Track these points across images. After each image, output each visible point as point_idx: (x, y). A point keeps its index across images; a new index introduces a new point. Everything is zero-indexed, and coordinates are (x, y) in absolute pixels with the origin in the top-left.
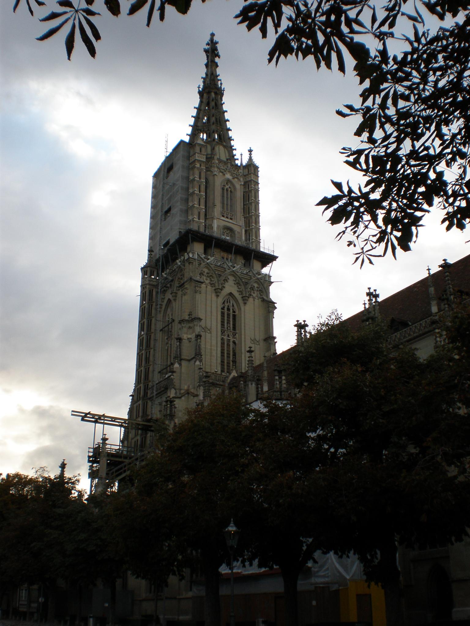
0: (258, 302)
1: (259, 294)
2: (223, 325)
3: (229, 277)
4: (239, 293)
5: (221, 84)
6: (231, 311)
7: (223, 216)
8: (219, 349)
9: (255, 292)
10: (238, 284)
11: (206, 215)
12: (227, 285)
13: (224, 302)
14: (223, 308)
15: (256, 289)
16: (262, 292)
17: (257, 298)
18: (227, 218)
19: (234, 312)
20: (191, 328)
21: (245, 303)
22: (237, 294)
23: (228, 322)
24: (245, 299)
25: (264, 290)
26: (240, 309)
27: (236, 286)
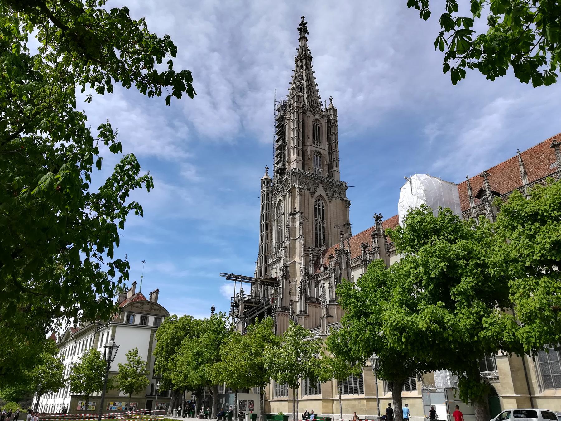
0: (339, 200)
2: (316, 216)
3: (319, 184)
5: (310, 53)
6: (321, 206)
7: (314, 144)
8: (314, 232)
10: (325, 189)
11: (303, 144)
12: (318, 190)
14: (316, 205)
18: (317, 145)
21: (330, 202)
22: (324, 196)
23: (319, 214)
24: (330, 199)
25: (342, 192)
26: (327, 205)
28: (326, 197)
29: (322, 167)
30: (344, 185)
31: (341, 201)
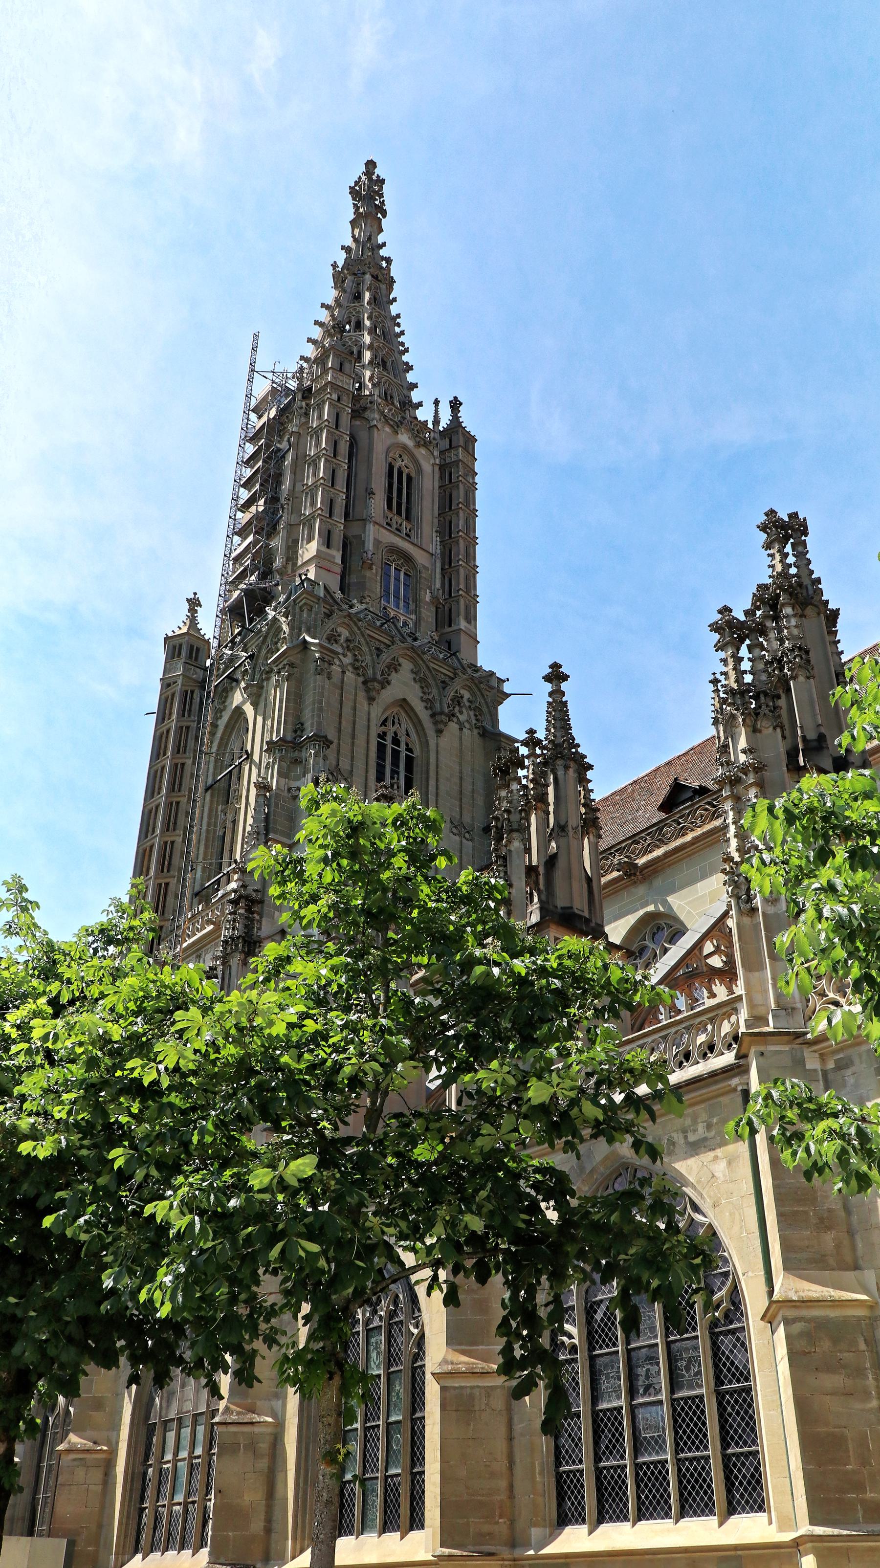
0: (470, 736)
1: (473, 718)
4: (424, 704)
6: (403, 746)
9: (464, 710)
11: (347, 515)
13: (386, 720)
14: (382, 736)
15: (467, 704)
16: (481, 712)
17: (466, 725)
19: (409, 750)
20: (301, 762)
21: (439, 732)
22: (419, 707)
23: (395, 773)
25: (485, 709)
26: (425, 744)
27: (417, 686)
28: (424, 715)
29: (412, 606)
30: (494, 683)
31: (478, 741)
